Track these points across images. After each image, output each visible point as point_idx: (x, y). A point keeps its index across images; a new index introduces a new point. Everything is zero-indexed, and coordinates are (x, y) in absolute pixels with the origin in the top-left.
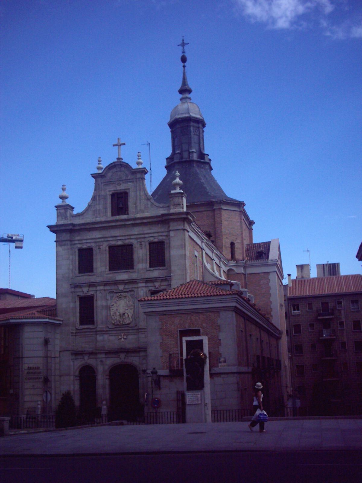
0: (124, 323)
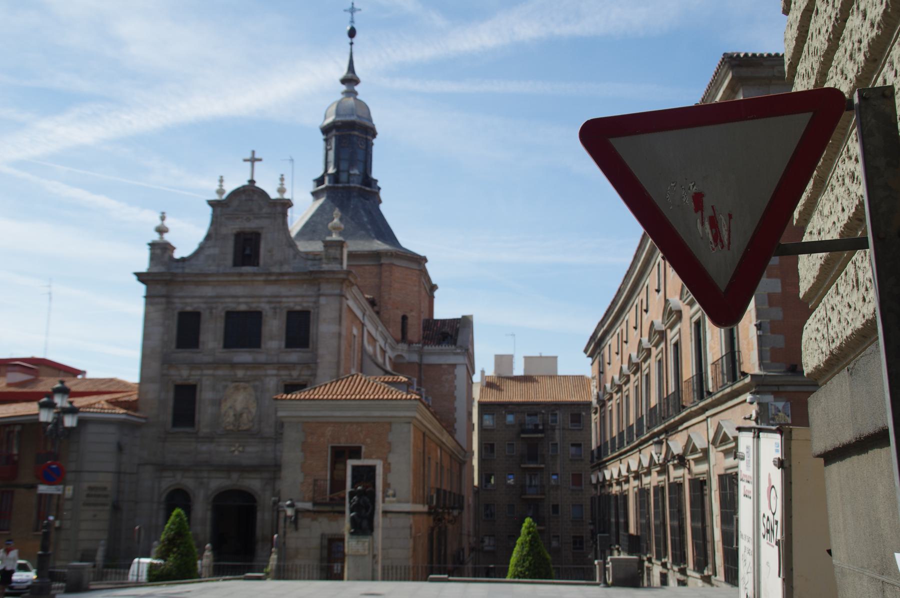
0: (240, 429)
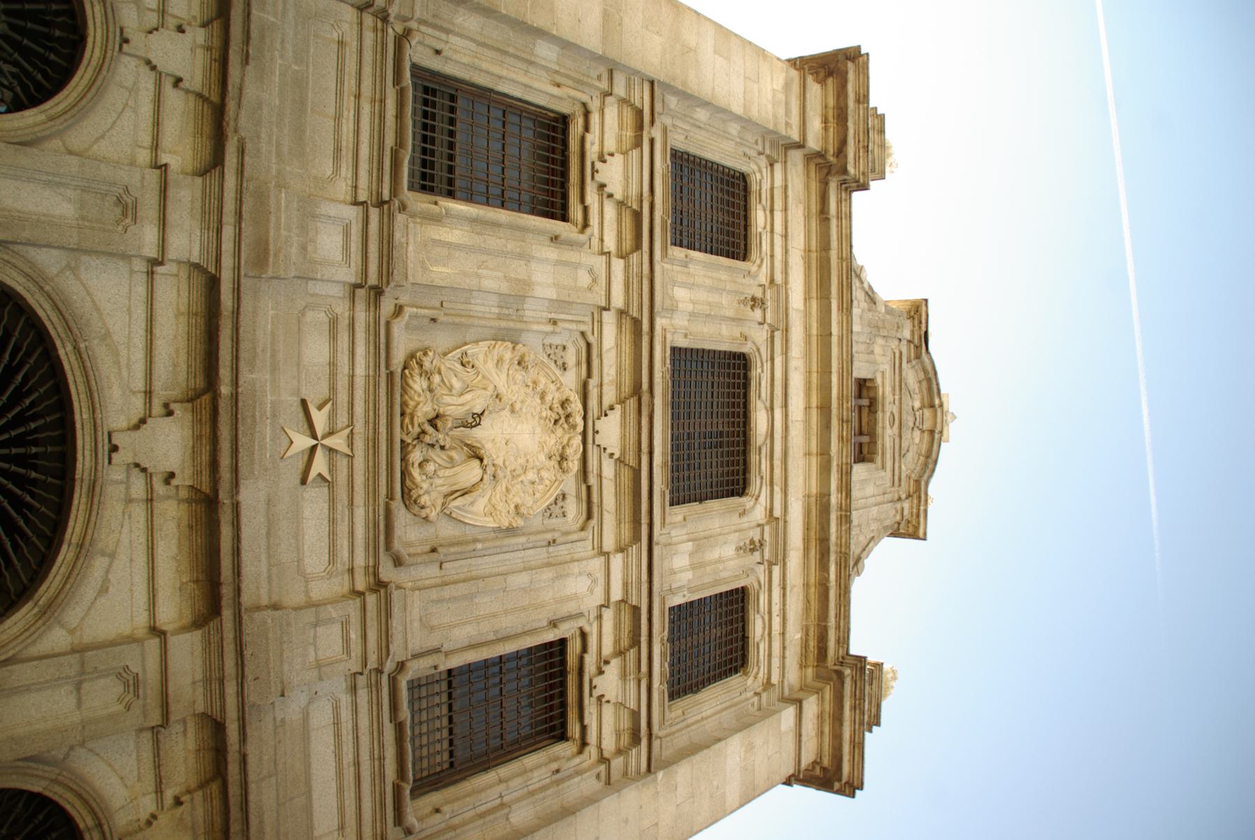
0: (416, 456)
